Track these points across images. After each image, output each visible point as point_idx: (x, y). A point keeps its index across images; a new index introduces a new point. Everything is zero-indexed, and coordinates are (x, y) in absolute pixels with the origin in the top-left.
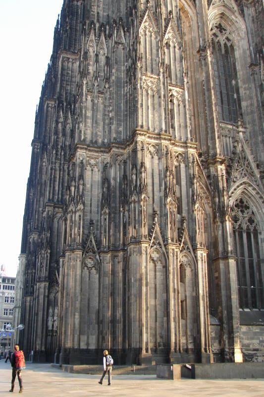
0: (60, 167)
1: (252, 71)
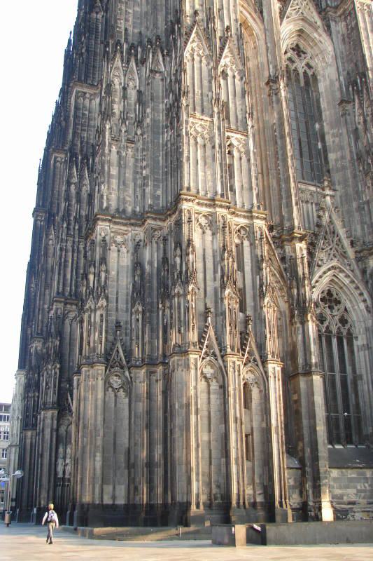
0: (73, 247)
1: (343, 110)
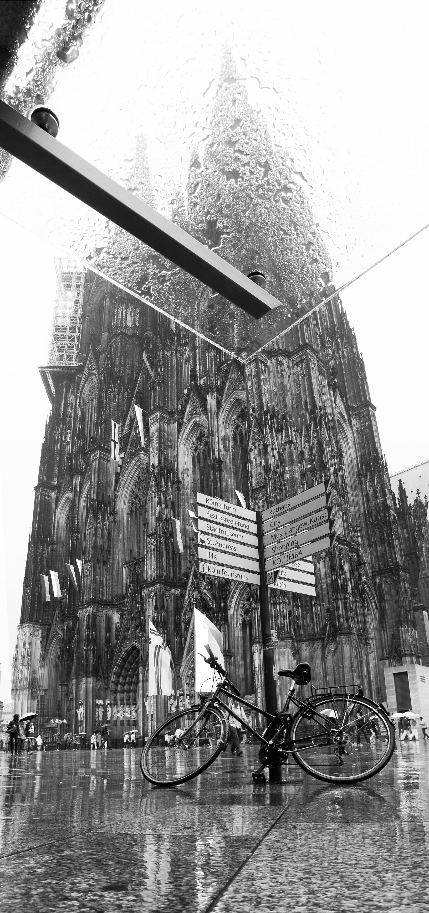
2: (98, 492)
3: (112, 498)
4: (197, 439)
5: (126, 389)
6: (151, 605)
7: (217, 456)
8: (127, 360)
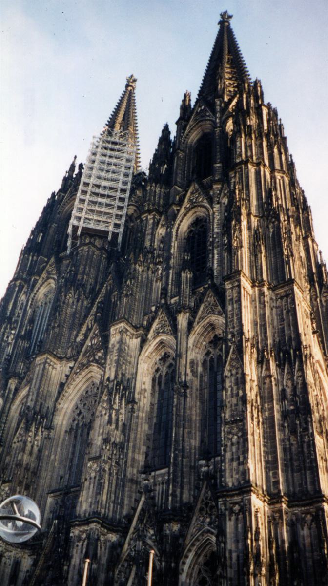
0: (110, 469)
2: (37, 401)
3: (51, 410)
4: (160, 360)
5: (87, 298)
6: (79, 551)
7: (183, 380)
8: (92, 270)
